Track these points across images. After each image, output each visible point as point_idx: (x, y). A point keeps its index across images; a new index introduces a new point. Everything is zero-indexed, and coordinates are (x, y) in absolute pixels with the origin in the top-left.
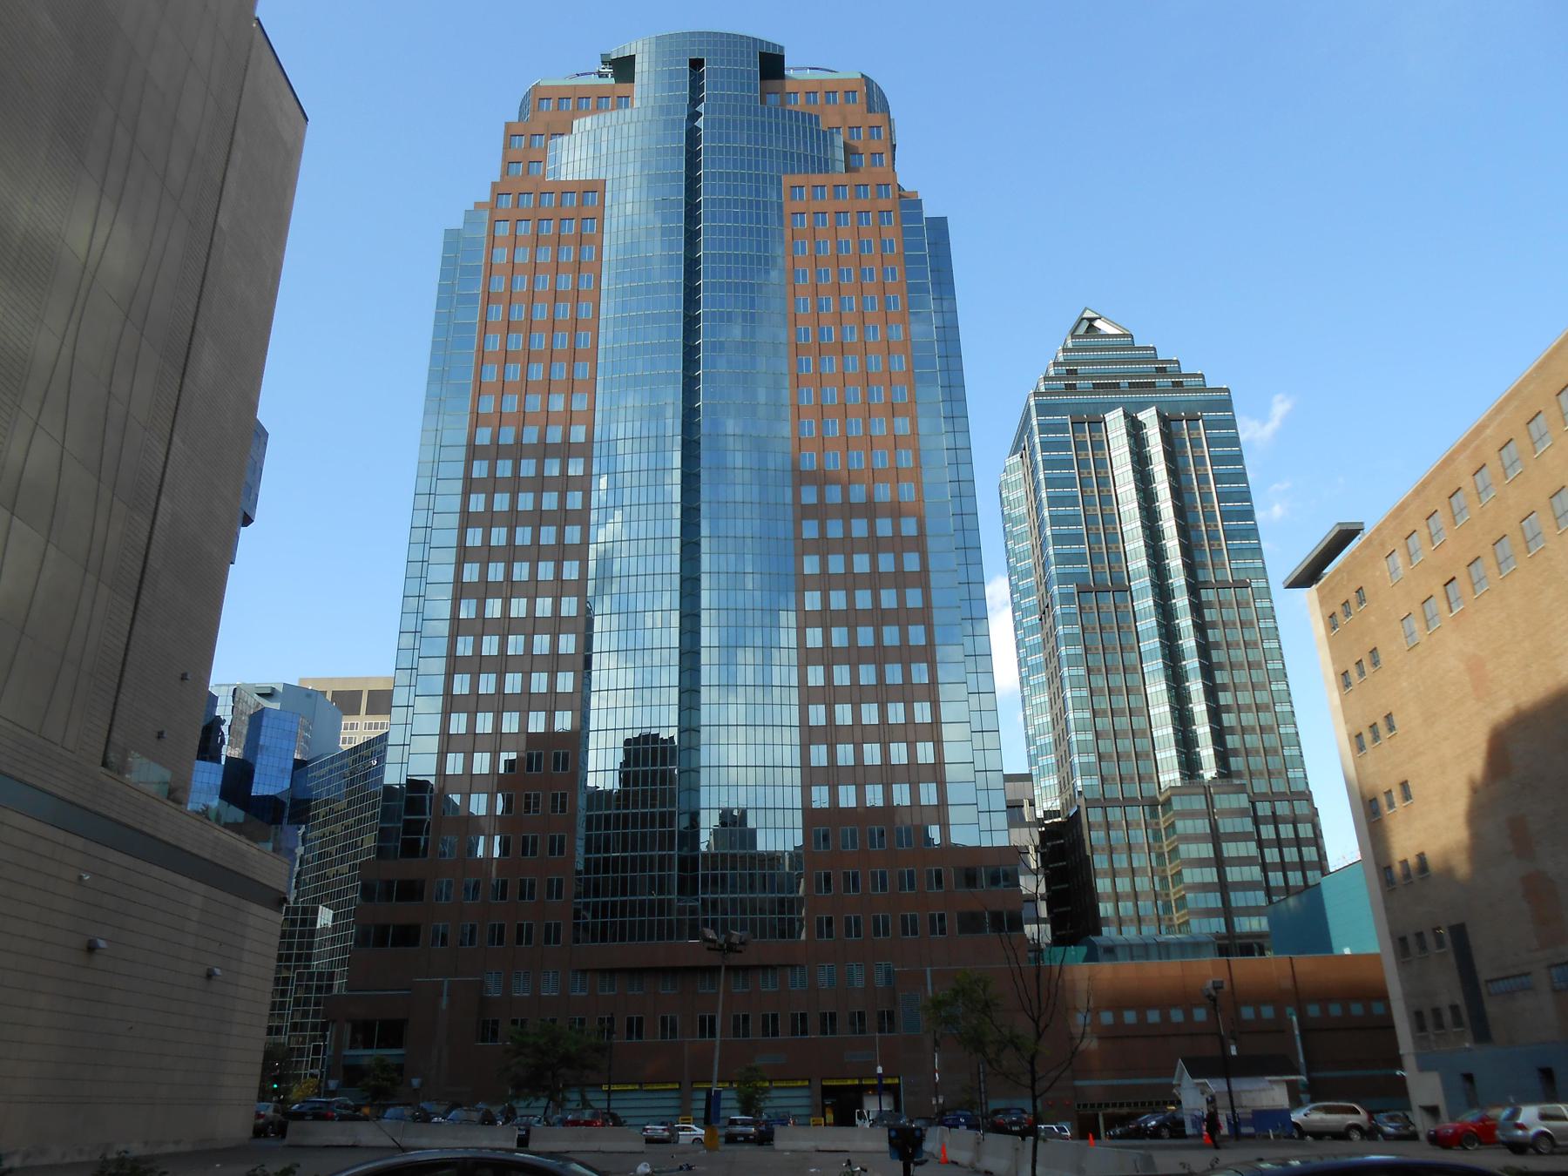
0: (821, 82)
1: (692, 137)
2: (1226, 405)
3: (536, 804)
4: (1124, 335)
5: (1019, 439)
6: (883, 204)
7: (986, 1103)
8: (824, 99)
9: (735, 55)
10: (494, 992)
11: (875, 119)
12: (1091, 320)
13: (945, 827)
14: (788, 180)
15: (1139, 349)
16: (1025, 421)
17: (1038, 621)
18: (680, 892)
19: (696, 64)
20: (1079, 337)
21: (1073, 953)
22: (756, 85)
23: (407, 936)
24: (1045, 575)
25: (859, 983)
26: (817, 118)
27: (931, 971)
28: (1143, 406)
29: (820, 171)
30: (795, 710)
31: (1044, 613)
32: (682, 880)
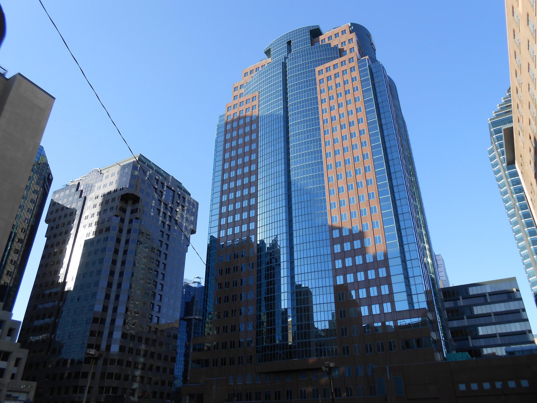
1: (284, 65)
14: (317, 69)
19: (289, 43)
21: (461, 355)
30: (330, 263)
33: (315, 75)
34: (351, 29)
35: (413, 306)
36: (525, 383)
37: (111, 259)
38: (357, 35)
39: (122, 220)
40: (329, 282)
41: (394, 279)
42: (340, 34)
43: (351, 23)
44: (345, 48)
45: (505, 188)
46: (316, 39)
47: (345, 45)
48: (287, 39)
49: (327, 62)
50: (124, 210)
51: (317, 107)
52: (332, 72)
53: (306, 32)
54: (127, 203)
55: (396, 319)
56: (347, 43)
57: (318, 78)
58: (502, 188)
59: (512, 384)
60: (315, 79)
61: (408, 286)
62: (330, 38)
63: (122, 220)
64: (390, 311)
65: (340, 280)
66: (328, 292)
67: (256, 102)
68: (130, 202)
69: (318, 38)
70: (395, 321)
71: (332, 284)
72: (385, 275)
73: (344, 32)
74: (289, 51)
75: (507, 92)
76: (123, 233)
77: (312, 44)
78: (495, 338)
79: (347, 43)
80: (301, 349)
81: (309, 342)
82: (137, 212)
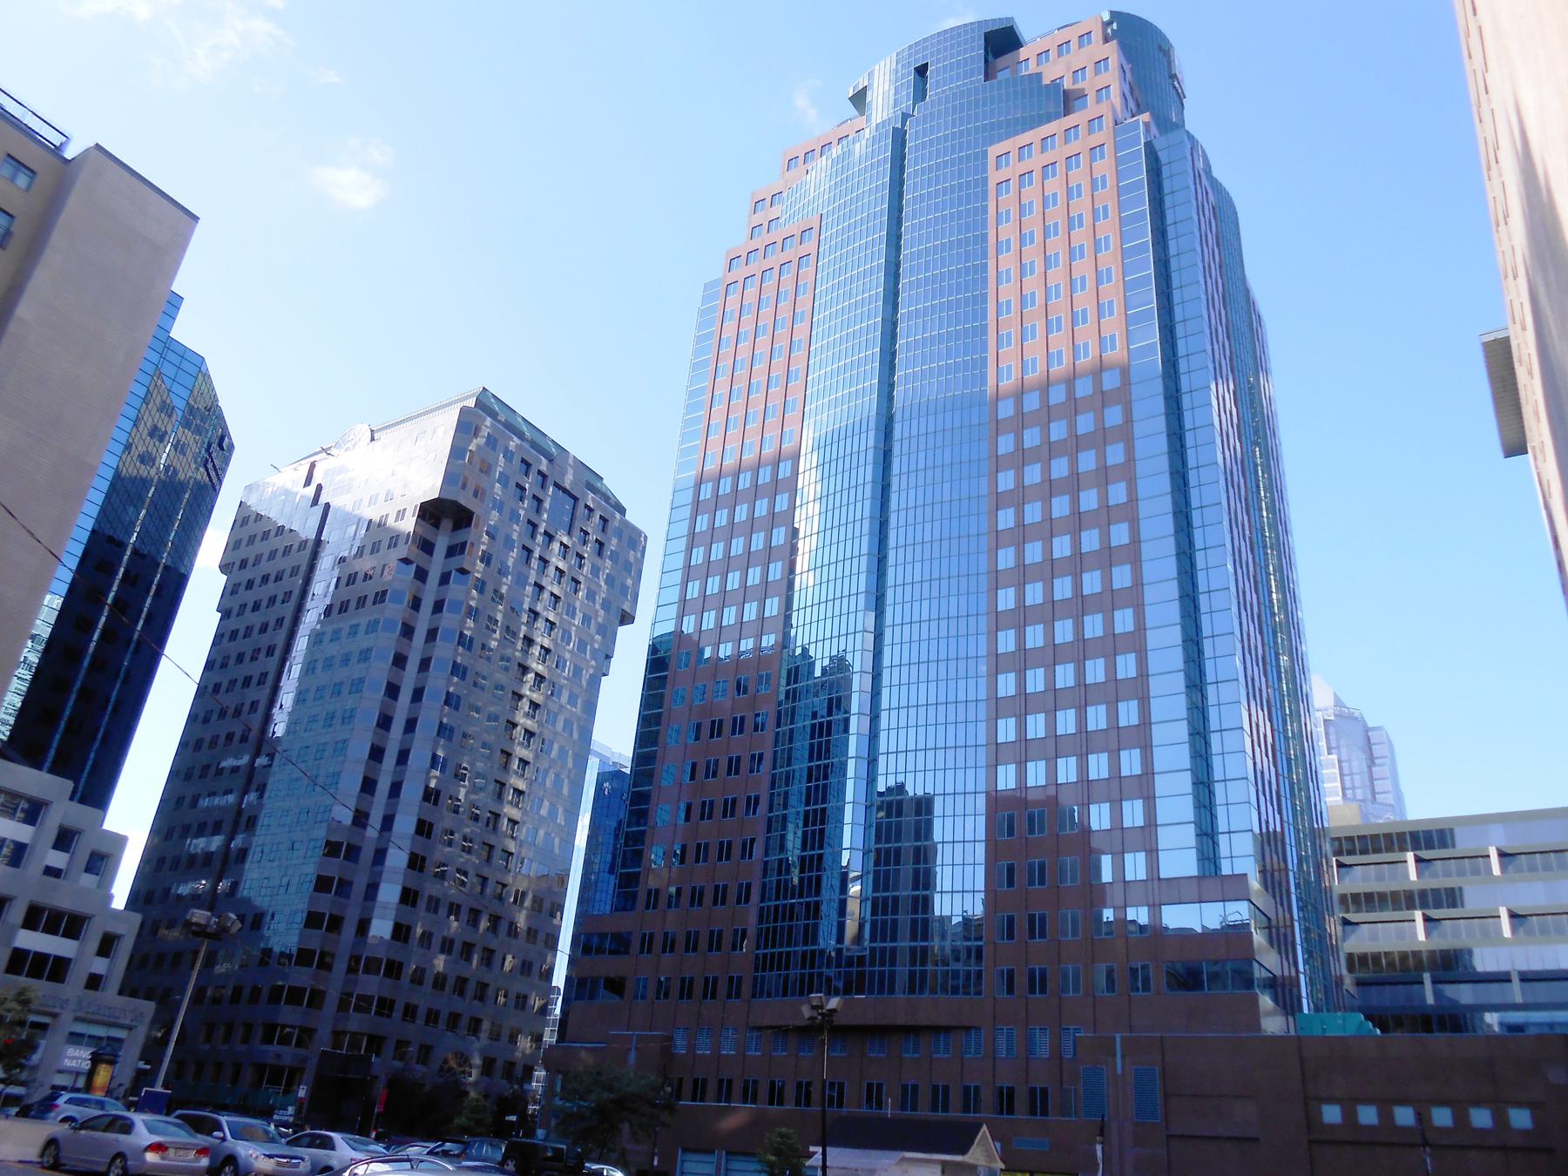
10: (681, 1046)
13: (1152, 852)
14: (994, 151)
19: (921, 71)
21: (1340, 1022)
23: (616, 986)
25: (1043, 1049)
27: (1123, 1039)
33: (985, 170)
34: (1109, 31)
35: (1217, 867)
36: (1520, 1118)
37: (385, 681)
38: (1127, 51)
39: (421, 575)
40: (975, 780)
41: (1161, 785)
42: (1074, 45)
43: (1112, 13)
46: (1003, 61)
48: (916, 60)
49: (1024, 131)
50: (427, 547)
51: (985, 266)
52: (1036, 161)
53: (973, 39)
54: (436, 525)
55: (1157, 902)
57: (994, 177)
59: (1481, 1118)
60: (985, 180)
61: (1205, 807)
62: (1043, 55)
63: (421, 575)
64: (1142, 875)
65: (1007, 779)
66: (970, 810)
67: (810, 246)
68: (447, 524)
70: (1155, 908)
71: (982, 787)
72: (1137, 770)
73: (1085, 37)
74: (920, 94)
76: (422, 608)
77: (988, 75)
78: (1506, 985)
80: (877, 968)
81: (894, 950)
82: (462, 551)
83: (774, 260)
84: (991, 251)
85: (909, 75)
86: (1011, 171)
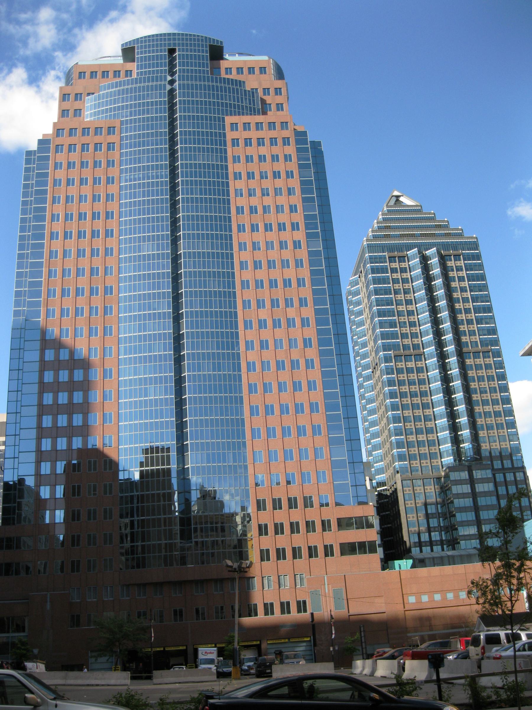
0: (245, 62)
2: (475, 245)
3: (95, 490)
4: (416, 206)
5: (358, 266)
6: (286, 133)
7: (366, 648)
8: (247, 72)
9: (195, 46)
11: (279, 84)
12: (397, 197)
14: (229, 120)
15: (425, 214)
16: (362, 255)
17: (371, 373)
18: (182, 538)
19: (172, 51)
20: (391, 206)
22: (207, 64)
24: (375, 347)
26: (244, 82)
28: (429, 246)
29: (247, 114)
31: (375, 368)
32: (182, 531)
44: (268, 99)
45: (364, 338)
47: (269, 94)
48: (169, 44)
56: (272, 91)
57: (230, 135)
58: (361, 338)
60: (225, 134)
62: (240, 70)
69: (217, 61)
73: (263, 70)
75: (385, 205)
79: (272, 91)
83: (91, 139)
84: (231, 176)
85: (165, 52)
86: (241, 134)
